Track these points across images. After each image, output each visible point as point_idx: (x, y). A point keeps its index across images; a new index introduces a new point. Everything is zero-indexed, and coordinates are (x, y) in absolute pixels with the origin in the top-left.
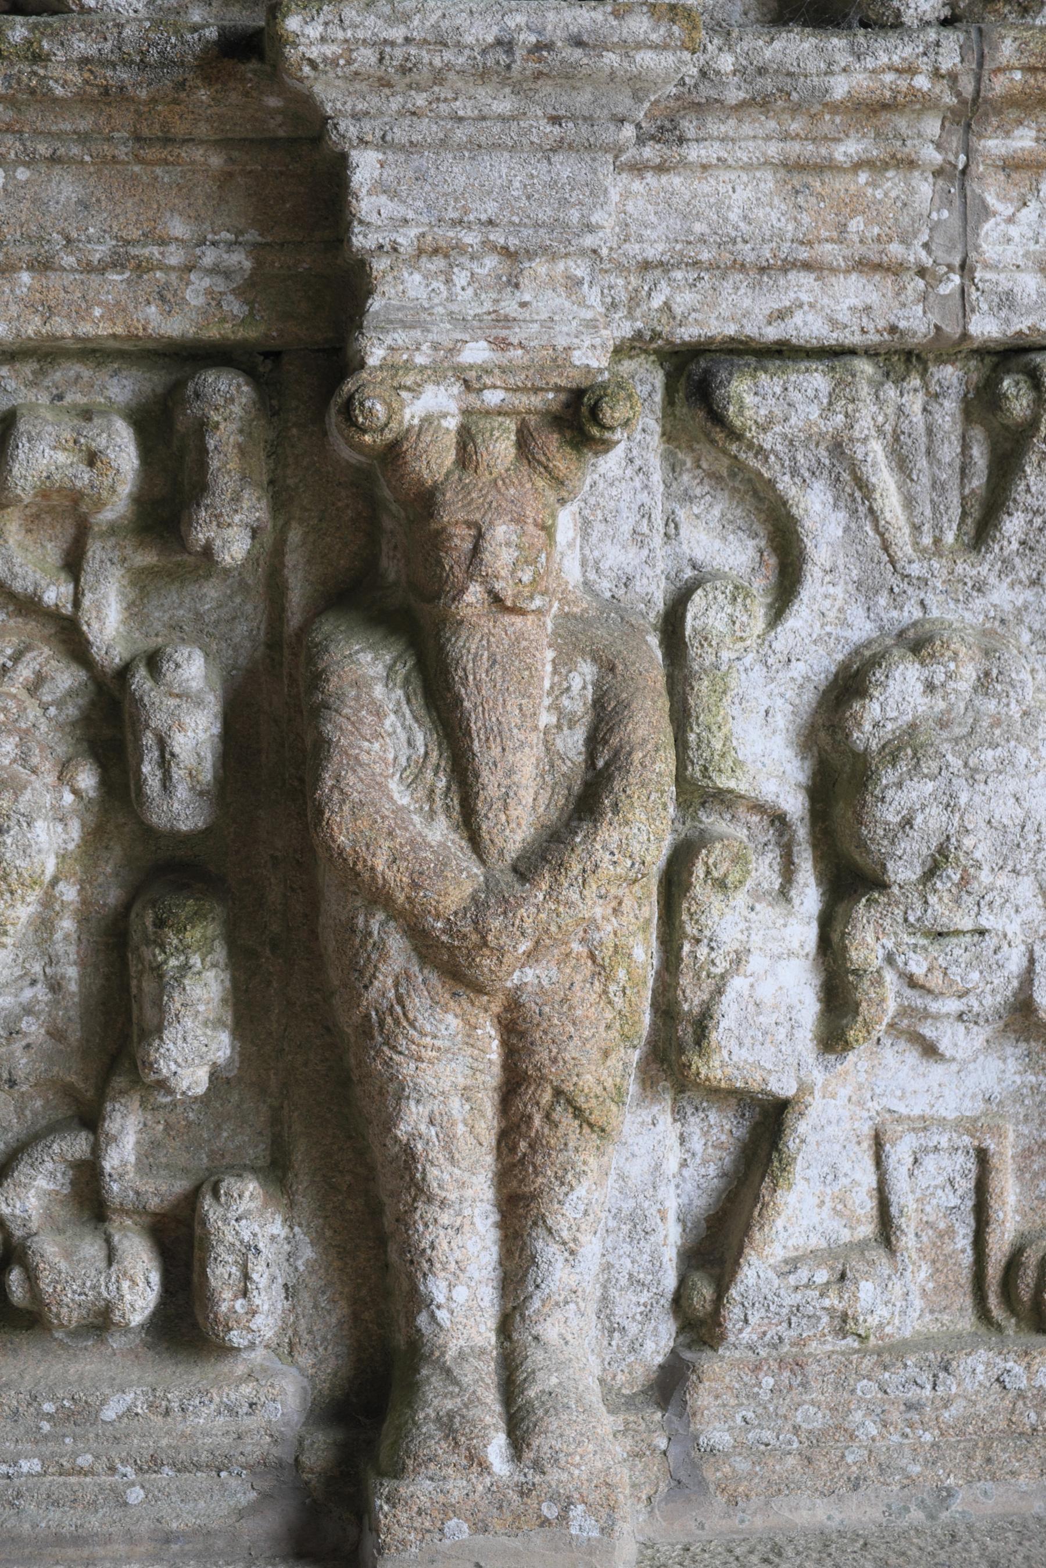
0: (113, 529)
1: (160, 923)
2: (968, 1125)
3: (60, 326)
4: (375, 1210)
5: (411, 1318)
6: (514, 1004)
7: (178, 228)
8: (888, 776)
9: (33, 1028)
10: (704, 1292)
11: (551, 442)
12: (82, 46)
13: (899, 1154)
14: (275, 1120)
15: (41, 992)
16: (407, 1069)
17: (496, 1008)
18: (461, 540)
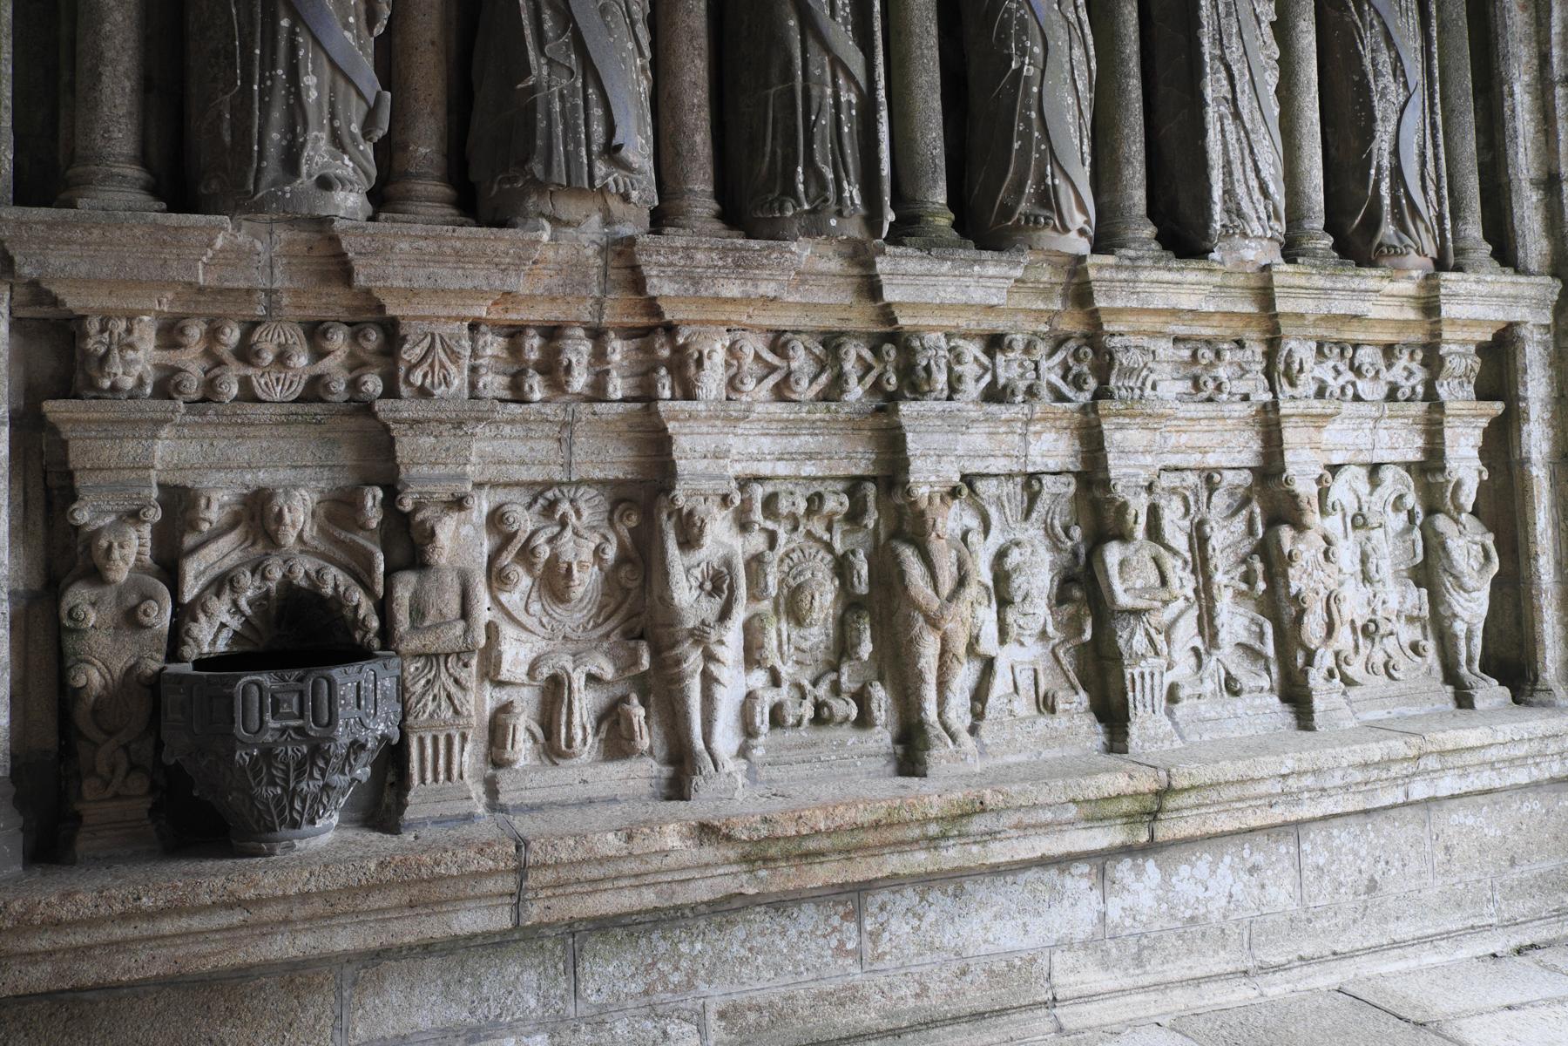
0: (839, 521)
1: (859, 617)
2: (1032, 663)
3: (834, 473)
4: (906, 689)
5: (919, 714)
6: (945, 633)
7: (860, 449)
8: (1014, 576)
9: (822, 646)
10: (979, 706)
11: (948, 499)
12: (847, 410)
13: (1017, 671)
14: (879, 667)
15: (824, 637)
16: (922, 650)
17: (941, 633)
18: (930, 522)
